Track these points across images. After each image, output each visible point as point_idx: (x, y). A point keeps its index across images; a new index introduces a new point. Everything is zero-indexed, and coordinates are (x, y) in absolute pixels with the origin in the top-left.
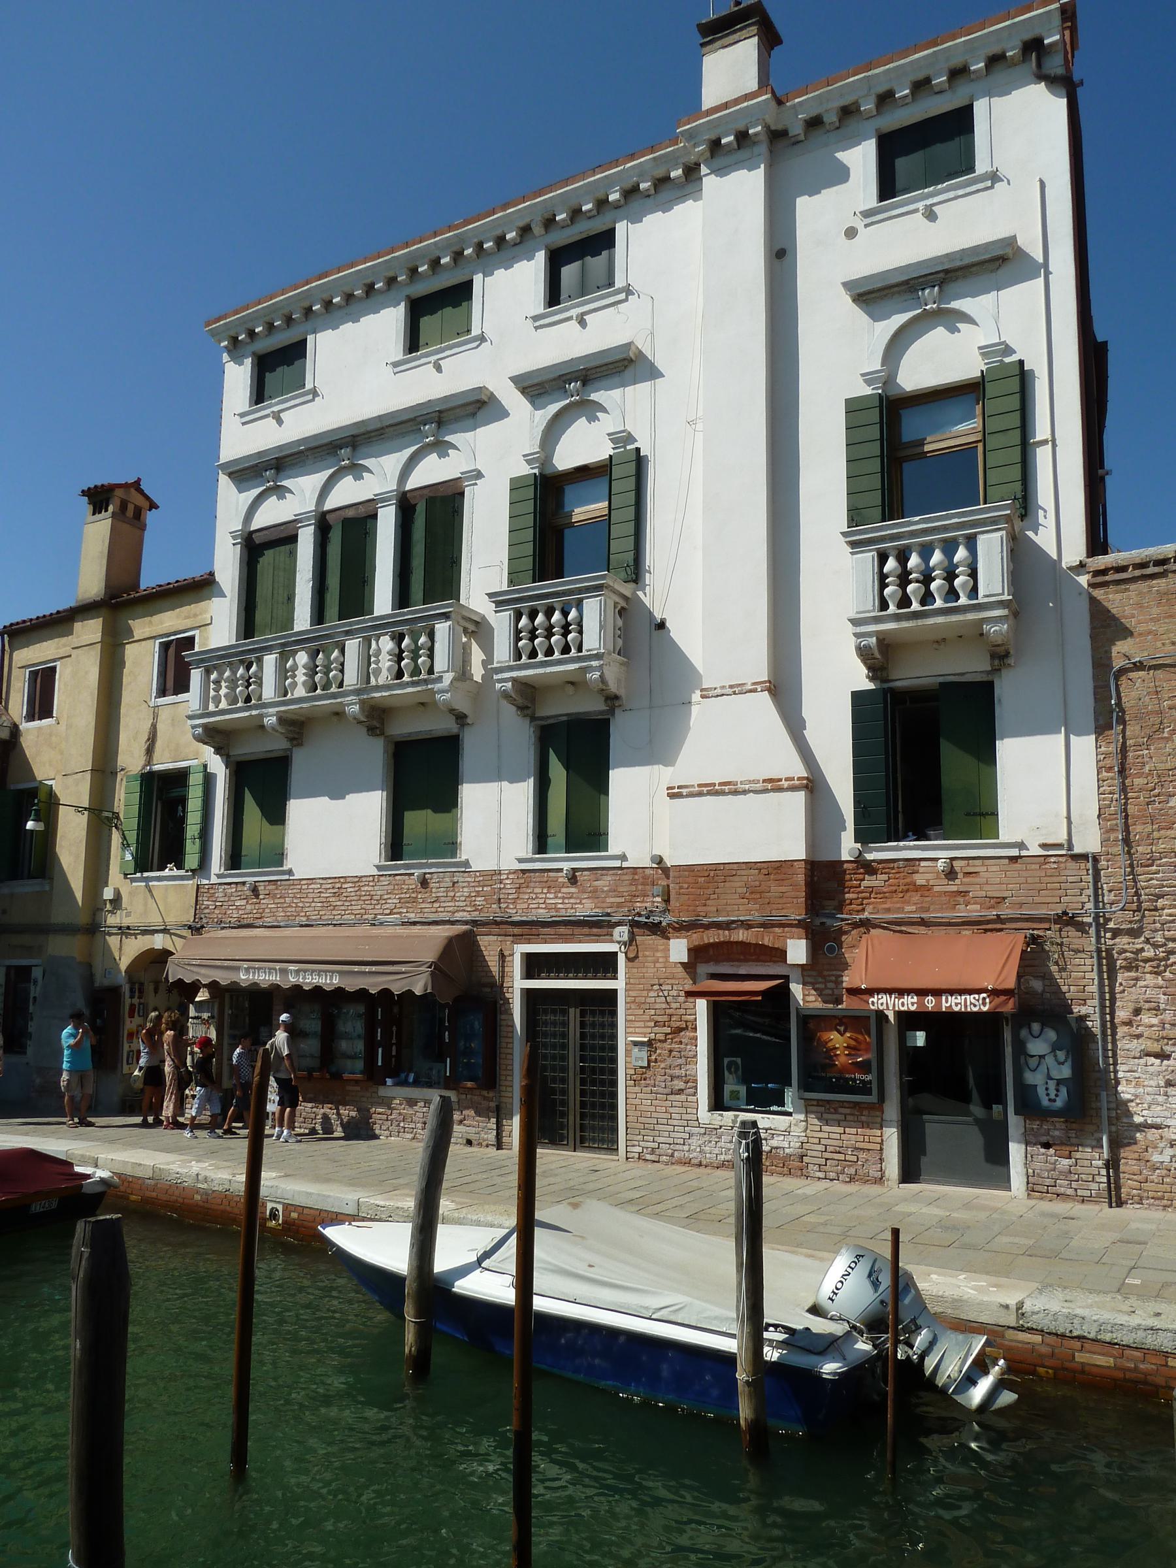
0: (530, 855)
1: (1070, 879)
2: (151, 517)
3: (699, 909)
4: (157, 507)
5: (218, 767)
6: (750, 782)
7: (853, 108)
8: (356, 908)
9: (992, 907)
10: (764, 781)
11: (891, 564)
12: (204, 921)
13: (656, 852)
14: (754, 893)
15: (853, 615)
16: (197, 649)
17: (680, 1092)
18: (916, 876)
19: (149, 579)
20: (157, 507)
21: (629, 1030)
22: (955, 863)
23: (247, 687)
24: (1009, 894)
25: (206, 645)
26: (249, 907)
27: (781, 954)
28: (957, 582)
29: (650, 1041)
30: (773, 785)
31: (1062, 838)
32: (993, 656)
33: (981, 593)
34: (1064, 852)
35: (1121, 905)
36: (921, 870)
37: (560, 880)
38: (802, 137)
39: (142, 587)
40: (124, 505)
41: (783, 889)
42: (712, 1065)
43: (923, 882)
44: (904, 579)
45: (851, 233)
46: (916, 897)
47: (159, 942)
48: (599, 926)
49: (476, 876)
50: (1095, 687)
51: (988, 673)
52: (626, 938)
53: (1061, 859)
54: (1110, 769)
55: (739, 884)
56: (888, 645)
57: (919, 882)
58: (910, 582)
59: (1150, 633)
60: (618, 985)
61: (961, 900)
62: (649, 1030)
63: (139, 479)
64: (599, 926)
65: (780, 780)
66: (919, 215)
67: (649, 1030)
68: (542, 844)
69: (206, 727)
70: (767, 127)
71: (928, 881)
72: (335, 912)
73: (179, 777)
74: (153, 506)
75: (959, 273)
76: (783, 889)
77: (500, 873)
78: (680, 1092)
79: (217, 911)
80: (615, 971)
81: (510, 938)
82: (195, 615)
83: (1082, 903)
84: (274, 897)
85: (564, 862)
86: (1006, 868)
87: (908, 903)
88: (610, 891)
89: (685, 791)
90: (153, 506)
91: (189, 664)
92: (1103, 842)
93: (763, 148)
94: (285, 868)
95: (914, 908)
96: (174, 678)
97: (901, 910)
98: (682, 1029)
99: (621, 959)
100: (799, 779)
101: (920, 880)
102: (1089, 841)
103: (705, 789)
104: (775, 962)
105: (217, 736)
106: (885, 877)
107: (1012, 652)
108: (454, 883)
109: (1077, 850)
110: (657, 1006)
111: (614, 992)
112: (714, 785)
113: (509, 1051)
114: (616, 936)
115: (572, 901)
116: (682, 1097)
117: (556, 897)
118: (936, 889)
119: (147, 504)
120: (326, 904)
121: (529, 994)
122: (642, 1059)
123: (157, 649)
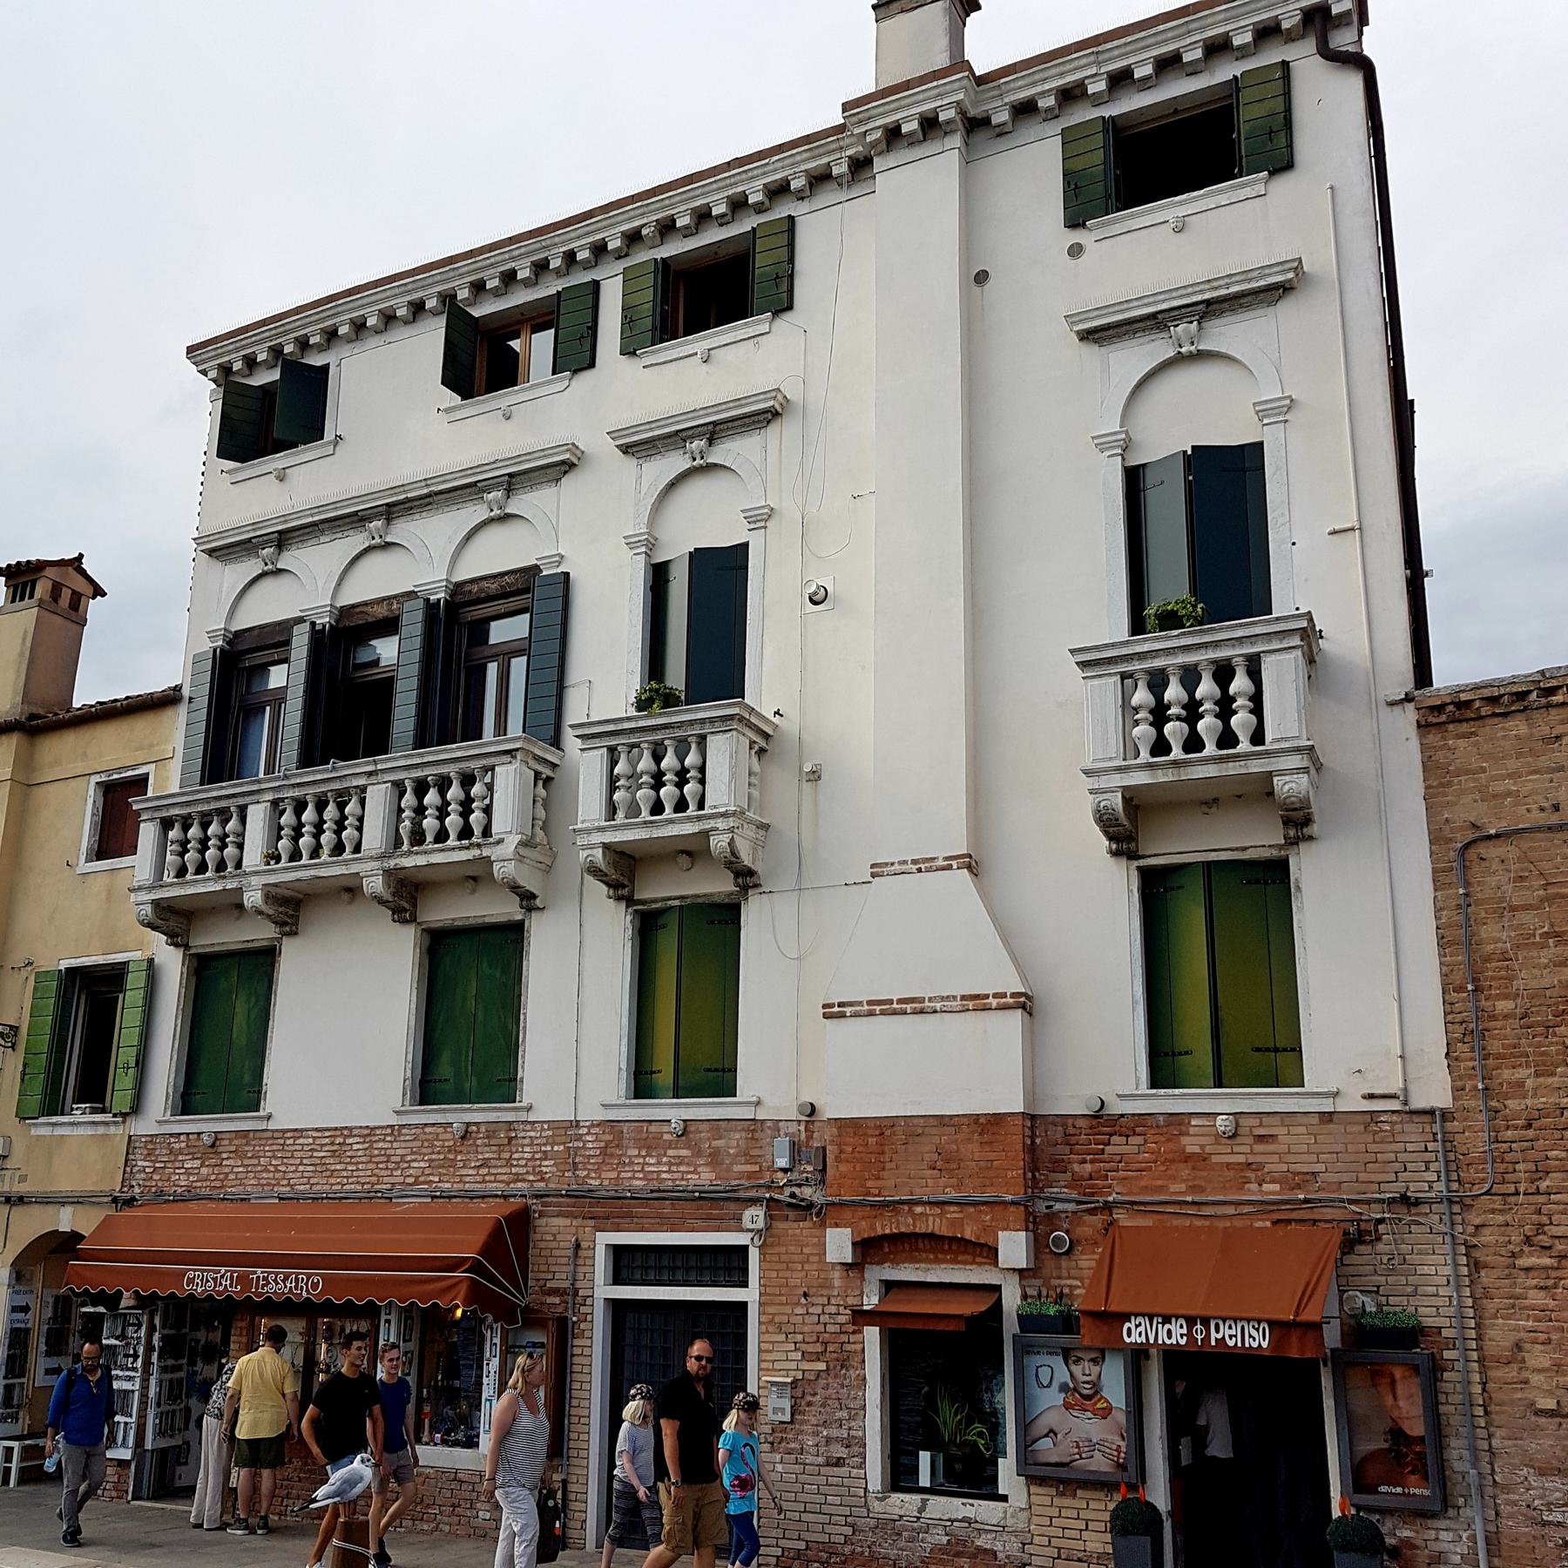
0: (622, 1101)
1: (1410, 1147)
2: (94, 607)
3: (869, 1184)
4: (104, 594)
5: (172, 963)
6: (942, 999)
7: (1077, 92)
8: (364, 1174)
9: (1298, 1187)
10: (963, 998)
11: (1142, 696)
12: (137, 1190)
13: (807, 1098)
14: (947, 1162)
15: (1089, 765)
16: (150, 794)
17: (839, 1462)
18: (1185, 1140)
19: (85, 695)
20: (104, 594)
21: (764, 1365)
22: (1243, 1122)
23: (182, 855)
24: (1320, 1167)
25: (166, 788)
26: (204, 1171)
27: (989, 1253)
28: (1201, 725)
29: (795, 1382)
30: (977, 1003)
31: (1395, 1086)
32: (1287, 822)
33: (1269, 737)
34: (1398, 1107)
35: (1487, 1186)
36: (1192, 1130)
37: (666, 1137)
38: (1009, 128)
39: (76, 704)
40: (56, 590)
41: (992, 1156)
42: (887, 1420)
43: (1197, 1149)
44: (1159, 715)
45: (1076, 251)
46: (1185, 1172)
47: (65, 1220)
48: (717, 1204)
49: (543, 1129)
50: (1434, 871)
51: (1280, 847)
52: (761, 1224)
53: (1395, 1118)
54: (1460, 989)
55: (927, 1148)
56: (1137, 807)
57: (1189, 1149)
58: (1169, 720)
59: (1509, 794)
60: (749, 1295)
61: (1252, 1175)
62: (793, 1365)
63: (81, 556)
64: (717, 1204)
65: (987, 997)
66: (1167, 228)
67: (793, 1365)
68: (642, 1086)
69: (156, 903)
70: (962, 113)
71: (1202, 1147)
72: (332, 1181)
73: (114, 976)
74: (98, 592)
75: (1226, 305)
76: (992, 1156)
77: (577, 1124)
78: (839, 1462)
79: (156, 1177)
80: (745, 1271)
81: (592, 1222)
82: (151, 746)
83: (1427, 1181)
84: (243, 1156)
85: (672, 1111)
86: (1315, 1130)
87: (1173, 1178)
88: (737, 1155)
89: (848, 1010)
90: (98, 592)
91: (138, 813)
92: (1457, 1090)
93: (956, 140)
94: (262, 1113)
95: (1183, 1187)
96: (113, 836)
97: (1161, 1189)
98: (846, 1361)
99: (754, 1255)
100: (1013, 995)
101: (1191, 1145)
102: (1435, 1091)
103: (878, 1008)
104: (980, 1264)
105: (174, 919)
106: (1139, 1140)
107: (1316, 817)
108: (510, 1139)
109: (1418, 1103)
110: (806, 1329)
111: (743, 1306)
112: (891, 1002)
113: (585, 1361)
114: (747, 1223)
115: (682, 1168)
116: (843, 1471)
117: (659, 1163)
118: (1215, 1159)
119: (90, 591)
120: (321, 1168)
121: (618, 1308)
122: (783, 1410)
123: (91, 792)
